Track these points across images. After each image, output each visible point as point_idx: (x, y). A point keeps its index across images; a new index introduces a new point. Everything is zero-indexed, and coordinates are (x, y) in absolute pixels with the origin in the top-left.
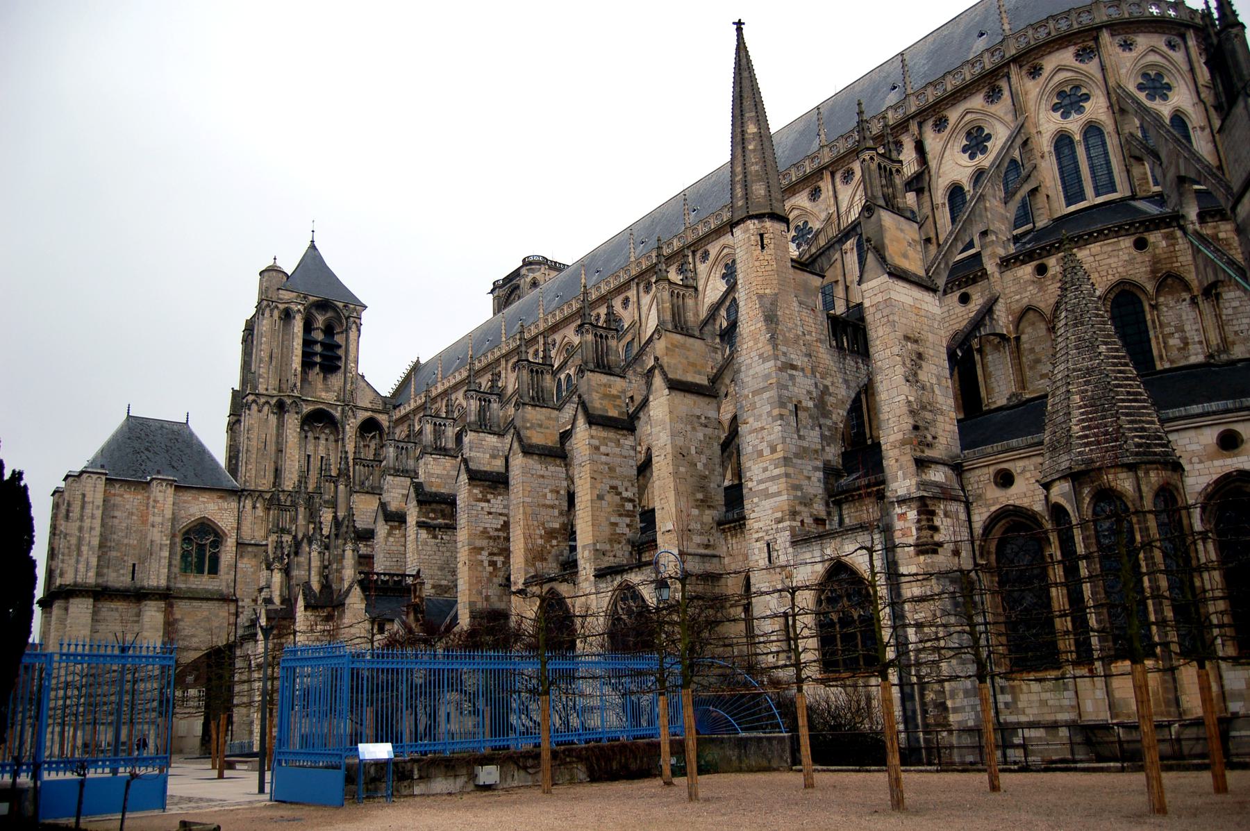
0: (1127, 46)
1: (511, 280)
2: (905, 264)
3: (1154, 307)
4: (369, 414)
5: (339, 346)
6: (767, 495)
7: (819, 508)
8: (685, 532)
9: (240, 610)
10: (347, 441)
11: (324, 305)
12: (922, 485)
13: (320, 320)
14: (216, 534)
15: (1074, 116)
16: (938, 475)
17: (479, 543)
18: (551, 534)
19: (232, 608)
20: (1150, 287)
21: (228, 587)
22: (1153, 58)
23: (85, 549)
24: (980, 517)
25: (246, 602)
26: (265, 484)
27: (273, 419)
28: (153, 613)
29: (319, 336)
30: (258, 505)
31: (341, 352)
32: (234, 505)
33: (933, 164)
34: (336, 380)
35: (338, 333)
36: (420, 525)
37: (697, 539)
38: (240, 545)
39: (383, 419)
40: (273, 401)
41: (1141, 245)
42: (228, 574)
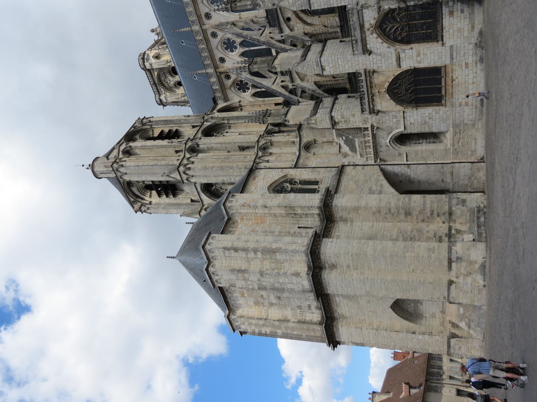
1: (155, 83)
9: (352, 164)
10: (230, 116)
14: (285, 182)
19: (348, 170)
21: (331, 171)
23: (274, 246)
25: (346, 161)
26: (250, 155)
27: (200, 155)
28: (344, 200)
30: (267, 159)
32: (262, 172)
35: (153, 134)
38: (296, 167)
40: (188, 155)
42: (319, 172)
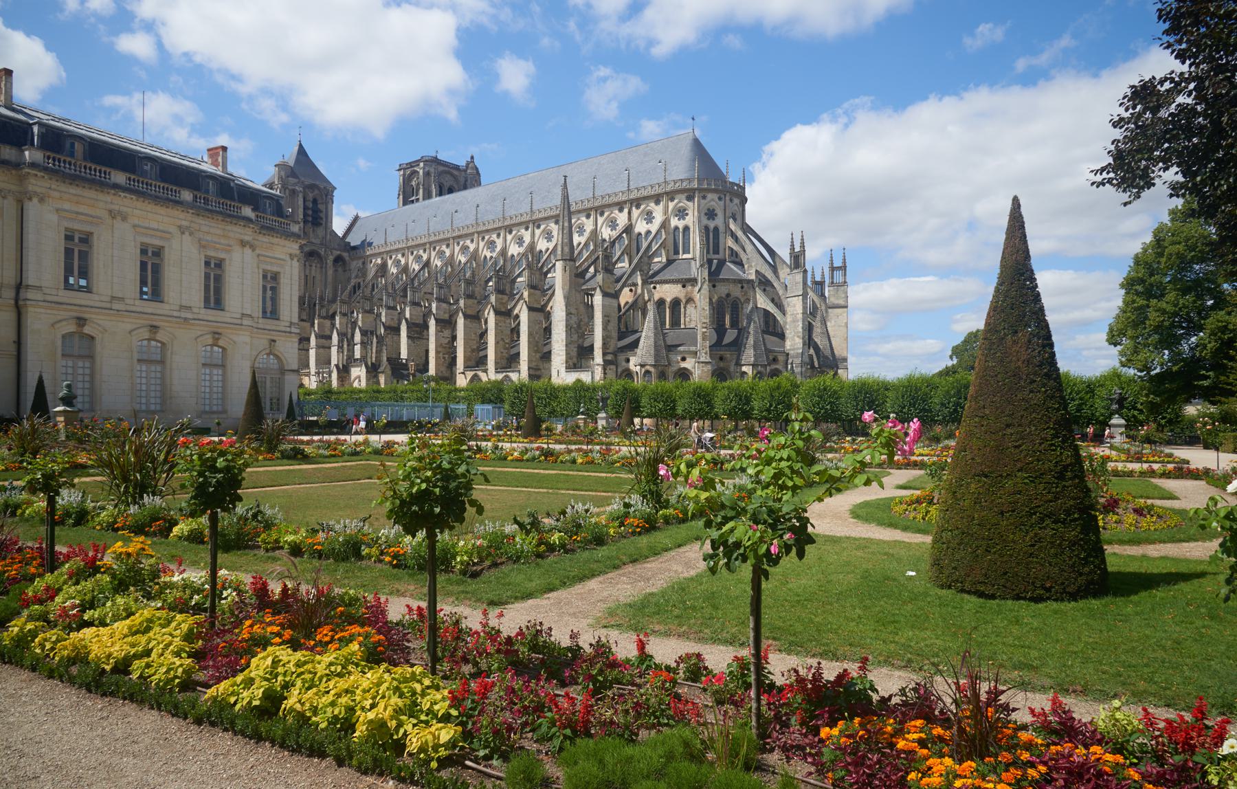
0: (704, 197)
2: (609, 291)
3: (685, 308)
4: (339, 252)
5: (321, 212)
6: (559, 355)
7: (575, 360)
8: (530, 361)
11: (312, 187)
12: (604, 361)
13: (311, 196)
15: (682, 221)
16: (609, 357)
17: (439, 349)
18: (473, 351)
20: (684, 301)
22: (713, 203)
24: (620, 370)
29: (311, 205)
31: (322, 215)
33: (634, 222)
34: (320, 231)
36: (409, 337)
37: (534, 364)
39: (345, 255)
41: (684, 286)
